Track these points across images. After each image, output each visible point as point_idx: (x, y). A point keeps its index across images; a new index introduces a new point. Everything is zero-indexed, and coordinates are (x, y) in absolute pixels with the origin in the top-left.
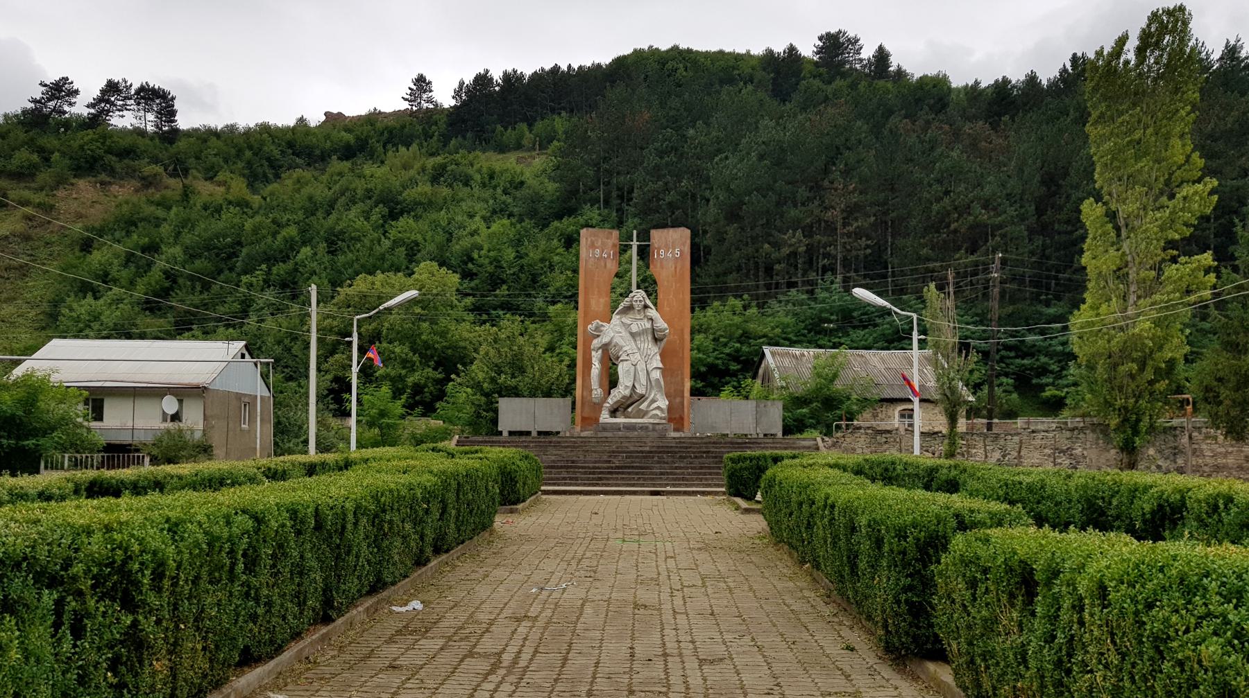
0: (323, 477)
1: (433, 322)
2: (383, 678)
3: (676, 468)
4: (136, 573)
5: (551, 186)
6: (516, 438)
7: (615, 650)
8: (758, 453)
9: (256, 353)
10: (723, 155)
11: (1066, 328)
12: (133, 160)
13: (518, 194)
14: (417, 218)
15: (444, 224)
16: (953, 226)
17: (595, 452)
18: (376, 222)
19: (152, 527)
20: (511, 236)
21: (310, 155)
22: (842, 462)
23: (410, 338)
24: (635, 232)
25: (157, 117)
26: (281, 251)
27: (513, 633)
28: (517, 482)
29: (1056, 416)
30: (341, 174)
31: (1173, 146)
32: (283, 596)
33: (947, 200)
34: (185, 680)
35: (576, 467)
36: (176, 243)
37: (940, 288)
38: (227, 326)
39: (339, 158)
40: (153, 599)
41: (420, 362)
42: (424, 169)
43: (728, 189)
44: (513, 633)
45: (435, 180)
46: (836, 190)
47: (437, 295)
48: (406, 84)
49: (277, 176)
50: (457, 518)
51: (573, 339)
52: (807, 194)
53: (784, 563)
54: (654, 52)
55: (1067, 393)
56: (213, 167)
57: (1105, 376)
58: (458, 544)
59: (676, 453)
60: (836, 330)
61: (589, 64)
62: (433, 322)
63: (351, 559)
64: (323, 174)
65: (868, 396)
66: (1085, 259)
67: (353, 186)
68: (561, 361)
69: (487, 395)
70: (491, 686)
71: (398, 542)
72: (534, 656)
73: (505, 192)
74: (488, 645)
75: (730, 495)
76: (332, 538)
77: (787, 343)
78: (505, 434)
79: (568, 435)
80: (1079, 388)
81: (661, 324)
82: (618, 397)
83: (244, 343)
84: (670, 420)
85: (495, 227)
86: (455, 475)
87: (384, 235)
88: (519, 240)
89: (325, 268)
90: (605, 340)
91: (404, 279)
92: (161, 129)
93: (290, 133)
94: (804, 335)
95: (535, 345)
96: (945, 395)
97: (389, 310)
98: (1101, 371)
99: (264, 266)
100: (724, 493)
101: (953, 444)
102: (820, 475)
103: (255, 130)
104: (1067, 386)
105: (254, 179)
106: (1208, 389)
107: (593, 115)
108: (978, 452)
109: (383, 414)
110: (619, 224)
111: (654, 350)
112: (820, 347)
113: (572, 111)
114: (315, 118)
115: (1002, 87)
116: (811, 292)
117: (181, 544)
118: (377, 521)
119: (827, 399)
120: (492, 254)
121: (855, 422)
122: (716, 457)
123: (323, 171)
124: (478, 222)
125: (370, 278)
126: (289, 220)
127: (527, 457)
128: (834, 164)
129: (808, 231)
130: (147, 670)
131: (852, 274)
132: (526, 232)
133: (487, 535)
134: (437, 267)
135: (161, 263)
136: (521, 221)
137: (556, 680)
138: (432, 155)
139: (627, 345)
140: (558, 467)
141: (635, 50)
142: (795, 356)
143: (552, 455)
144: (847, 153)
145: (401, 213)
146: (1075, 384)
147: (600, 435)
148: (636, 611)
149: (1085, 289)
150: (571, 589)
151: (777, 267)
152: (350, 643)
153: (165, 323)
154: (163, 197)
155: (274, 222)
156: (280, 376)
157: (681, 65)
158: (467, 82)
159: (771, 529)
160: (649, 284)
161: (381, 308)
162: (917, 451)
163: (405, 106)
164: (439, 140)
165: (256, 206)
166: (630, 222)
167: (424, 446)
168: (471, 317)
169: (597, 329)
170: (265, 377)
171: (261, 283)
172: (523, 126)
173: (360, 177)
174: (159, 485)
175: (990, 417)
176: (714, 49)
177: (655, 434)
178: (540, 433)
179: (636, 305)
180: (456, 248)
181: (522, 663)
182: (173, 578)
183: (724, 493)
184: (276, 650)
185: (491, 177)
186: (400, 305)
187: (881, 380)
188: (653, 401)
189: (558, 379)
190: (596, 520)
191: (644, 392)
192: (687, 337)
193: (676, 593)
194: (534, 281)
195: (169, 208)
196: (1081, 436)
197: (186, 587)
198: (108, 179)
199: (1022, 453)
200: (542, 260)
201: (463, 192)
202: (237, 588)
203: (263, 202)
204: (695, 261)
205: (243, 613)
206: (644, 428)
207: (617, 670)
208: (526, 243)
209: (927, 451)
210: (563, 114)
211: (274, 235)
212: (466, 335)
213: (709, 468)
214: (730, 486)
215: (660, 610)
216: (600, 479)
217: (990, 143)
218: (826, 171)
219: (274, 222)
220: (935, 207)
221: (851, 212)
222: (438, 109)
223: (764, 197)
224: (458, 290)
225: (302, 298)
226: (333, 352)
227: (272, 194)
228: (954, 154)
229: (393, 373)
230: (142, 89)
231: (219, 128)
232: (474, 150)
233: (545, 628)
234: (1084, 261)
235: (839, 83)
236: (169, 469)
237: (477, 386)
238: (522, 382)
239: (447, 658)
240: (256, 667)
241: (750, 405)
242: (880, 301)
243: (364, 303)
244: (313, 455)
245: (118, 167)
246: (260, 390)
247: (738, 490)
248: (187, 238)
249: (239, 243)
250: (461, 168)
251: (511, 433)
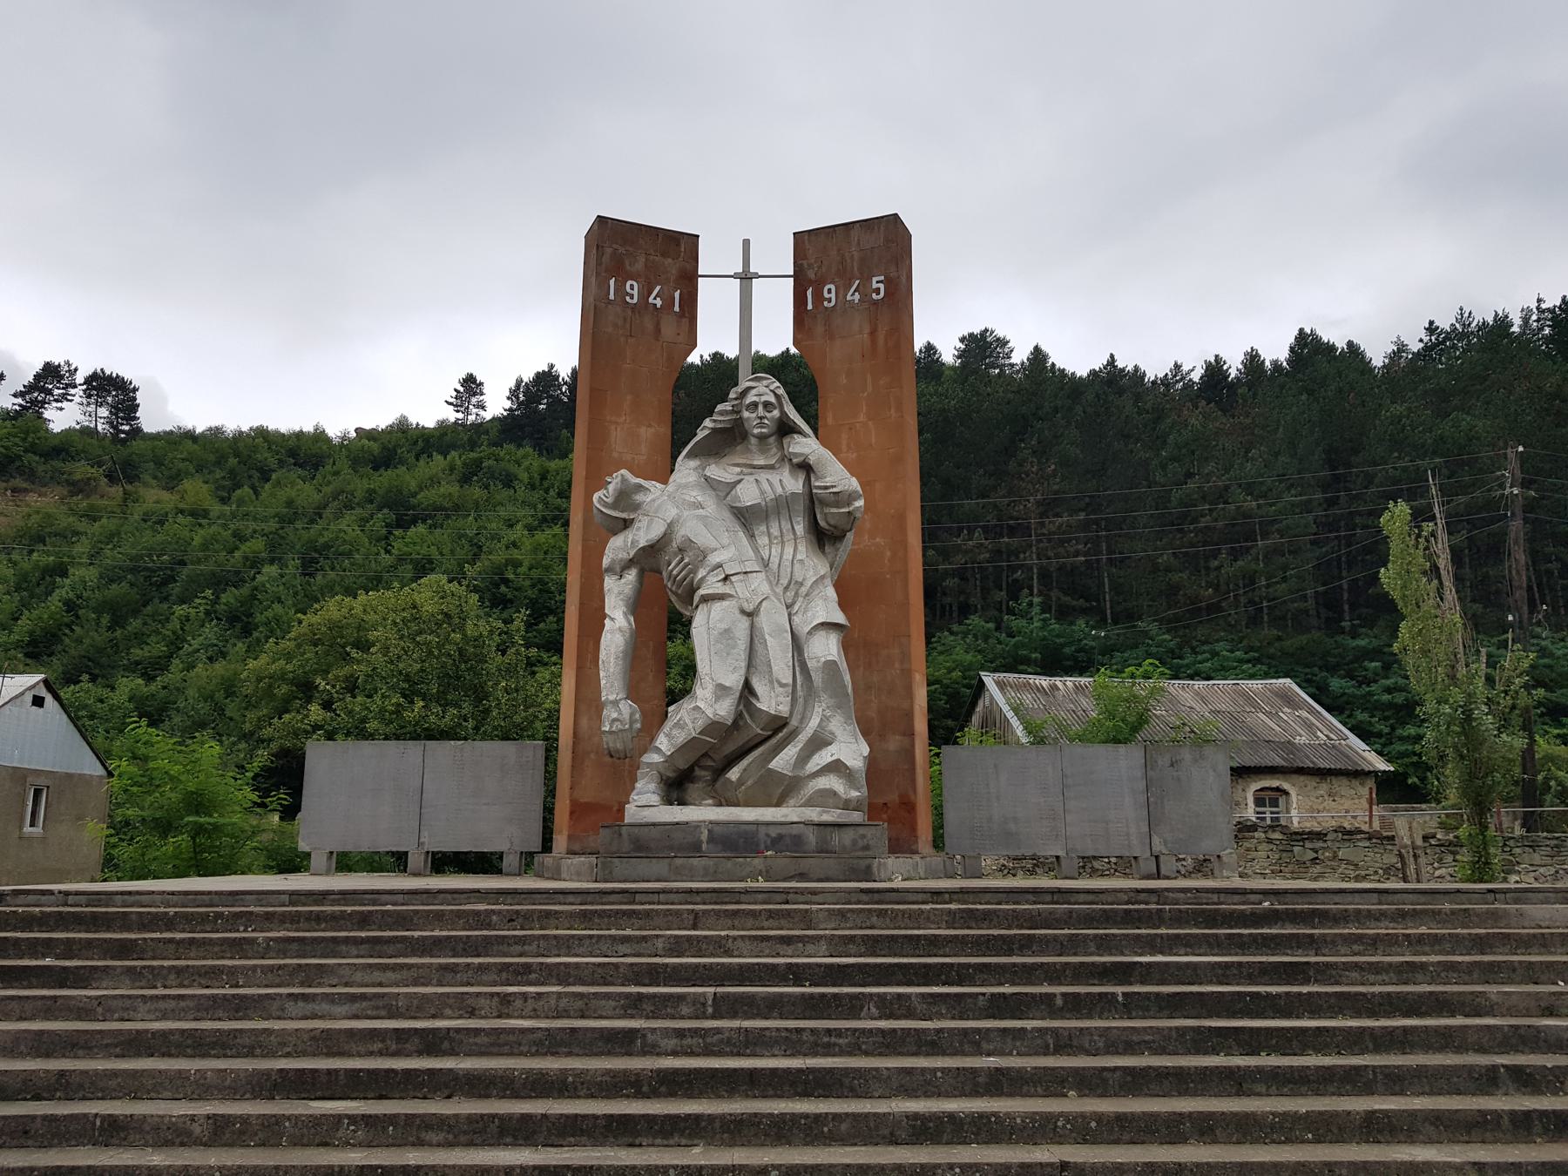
12: (64, 460)
26: (237, 573)
45: (465, 480)
99: (209, 592)
124: (519, 531)
145: (414, 522)
154: (92, 507)
171: (201, 615)
185: (543, 477)
198: (25, 485)
248: (111, 556)
250: (502, 464)
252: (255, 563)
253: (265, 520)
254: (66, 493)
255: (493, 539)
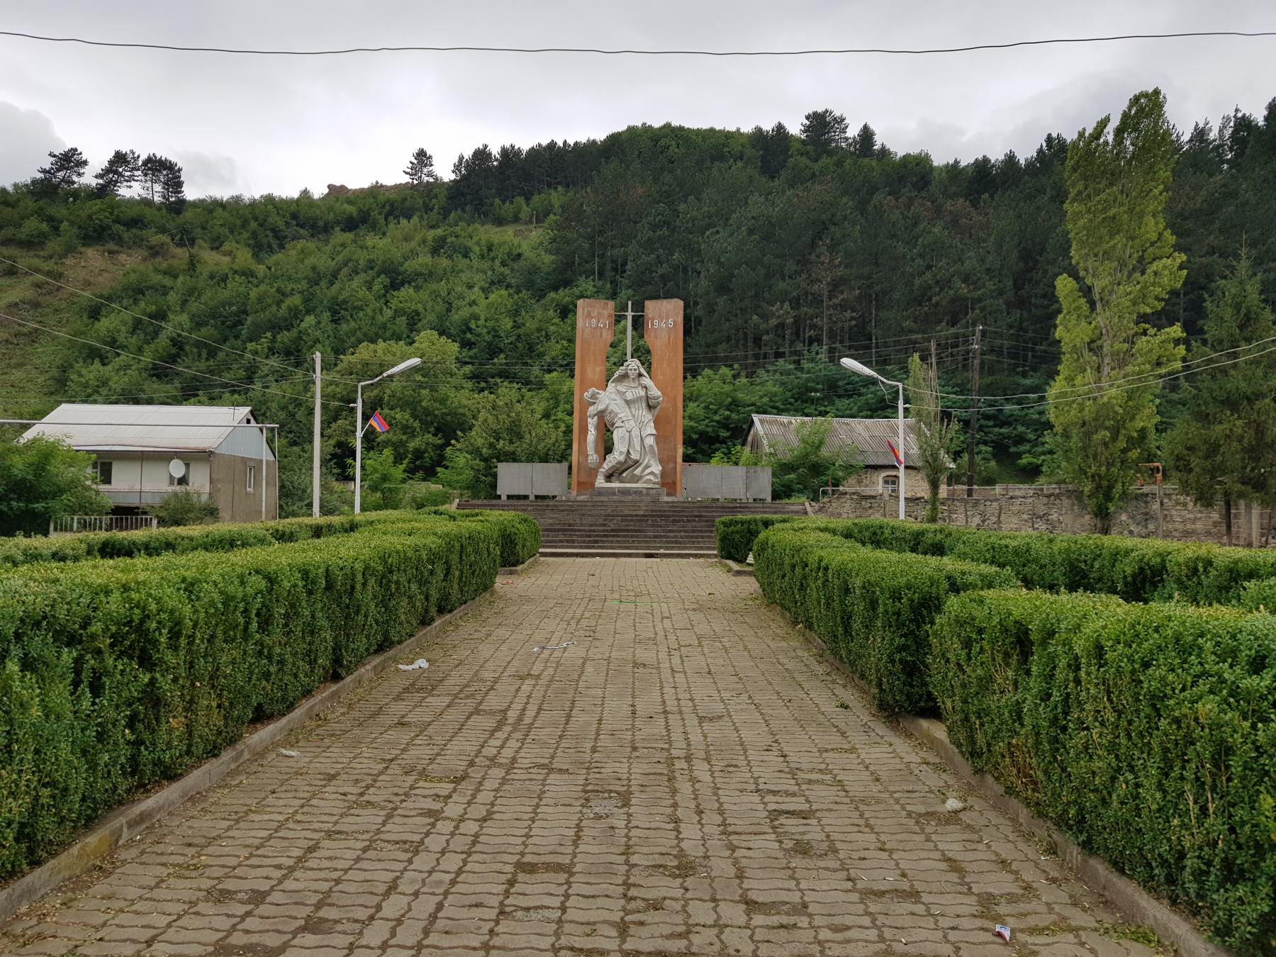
0: (331, 539)
1: (433, 389)
2: (392, 735)
3: (670, 531)
4: (154, 631)
5: (548, 259)
6: (514, 502)
7: (617, 709)
8: (749, 517)
9: (261, 418)
10: (714, 230)
11: (1042, 398)
12: (141, 229)
13: (516, 266)
14: (417, 288)
15: (444, 294)
16: (934, 300)
17: (590, 515)
18: (378, 291)
19: (169, 587)
20: (509, 306)
21: (313, 226)
22: (831, 526)
23: (410, 404)
24: (630, 303)
25: (164, 188)
26: (286, 320)
27: (518, 690)
28: (516, 544)
29: (1033, 483)
30: (343, 245)
31: (1146, 224)
32: (295, 654)
33: (928, 275)
34: (200, 737)
35: (573, 530)
36: (183, 311)
37: (923, 359)
38: (233, 392)
39: (342, 230)
40: (170, 658)
41: (421, 428)
42: (424, 241)
43: (718, 261)
44: (518, 690)
45: (435, 251)
46: (822, 263)
47: (437, 363)
48: (406, 159)
49: (282, 247)
50: (460, 579)
51: (568, 407)
52: (795, 268)
53: (777, 624)
54: (647, 129)
55: (1044, 461)
56: (219, 238)
57: (1080, 445)
58: (461, 604)
59: (669, 516)
60: (822, 399)
61: (584, 141)
62: (433, 389)
63: (360, 618)
64: (326, 245)
65: (854, 462)
66: (1059, 332)
67: (356, 257)
68: (557, 428)
69: (486, 460)
70: (498, 743)
71: (405, 601)
72: (538, 713)
73: (503, 264)
74: (493, 702)
75: (722, 557)
76: (341, 598)
77: (775, 411)
78: (504, 498)
79: (564, 498)
80: (1055, 456)
81: (655, 392)
82: (614, 463)
83: (249, 409)
84: (663, 485)
85: (492, 297)
86: (459, 537)
87: (385, 304)
88: (517, 311)
89: (329, 336)
90: (601, 407)
91: (405, 347)
92: (168, 199)
93: (295, 205)
94: (791, 404)
95: (533, 412)
96: (927, 462)
97: (391, 377)
98: (1075, 442)
99: (269, 334)
100: (716, 556)
101: (934, 509)
102: (812, 538)
103: (260, 202)
104: (1044, 453)
105: (259, 249)
106: (1178, 458)
107: (589, 190)
108: (960, 519)
109: (385, 478)
110: (613, 296)
111: (648, 417)
112: (807, 416)
113: (568, 186)
114: (319, 191)
115: (982, 166)
116: (798, 362)
117: (197, 604)
118: (384, 581)
119: (814, 466)
120: (490, 324)
121: (841, 488)
122: (707, 521)
123: (327, 242)
125: (372, 346)
126: (293, 290)
127: (525, 521)
128: (821, 239)
129: (795, 304)
130: (164, 727)
131: (838, 345)
132: (524, 302)
133: (487, 595)
134: (437, 337)
135: (169, 330)
136: (518, 292)
137: (561, 737)
138: (432, 227)
139: (622, 413)
140: (554, 530)
141: (629, 128)
142: (783, 424)
143: (549, 519)
144: (833, 228)
145: (403, 284)
146: (1051, 452)
147: (595, 499)
148: (636, 670)
149: (1059, 362)
150: (572, 649)
151: (765, 337)
152: (359, 700)
153: (172, 388)
155: (278, 291)
156: (284, 441)
157: (673, 142)
158: (466, 157)
159: (764, 590)
160: (643, 353)
161: (385, 375)
162: (902, 516)
163: (406, 179)
164: (439, 213)
165: (261, 275)
166: (624, 293)
167: (427, 509)
168: (469, 384)
169: (594, 396)
170: (270, 442)
172: (520, 200)
173: (362, 248)
174: (170, 546)
175: (970, 483)
176: (705, 126)
177: (648, 499)
178: (537, 497)
179: (632, 374)
180: (456, 317)
181: (527, 721)
182: (189, 637)
183: (716, 556)
184: (288, 707)
185: (490, 250)
186: (402, 373)
187: (866, 447)
188: (647, 467)
189: (554, 445)
190: (592, 581)
191: (638, 458)
192: (680, 404)
193: (673, 652)
194: (531, 349)
195: (175, 277)
196: (1058, 502)
197: (202, 646)
199: (1002, 519)
200: (539, 330)
201: (462, 263)
202: (251, 647)
203: (267, 270)
204: (687, 332)
205: (256, 671)
206: (638, 492)
207: (619, 727)
208: (523, 313)
209: (910, 516)
210: (560, 188)
211: (279, 304)
212: (465, 402)
213: (701, 531)
214: (722, 550)
215: (658, 668)
216: (596, 542)
217: (971, 220)
218: (813, 245)
219: (278, 291)
220: (917, 282)
221: (836, 286)
222: (438, 183)
223: (754, 270)
224: (457, 358)
225: (306, 365)
226: (335, 419)
227: (277, 264)
228: (936, 230)
229: (395, 439)
230: (149, 160)
231: (225, 199)
232: (473, 223)
233: (548, 686)
234: (1057, 335)
235: (825, 160)
236: (180, 530)
237: (476, 452)
238: (519, 447)
239: (454, 715)
240: (268, 724)
241: (740, 471)
242: (867, 371)
243: (366, 370)
244: (317, 518)
245: (125, 236)
246: (266, 455)
247: (729, 553)
248: (194, 306)
249: (245, 312)
250: (461, 239)
251: (509, 497)
252: (296, 315)
253: (297, 281)
254: (146, 254)
255: (459, 298)
